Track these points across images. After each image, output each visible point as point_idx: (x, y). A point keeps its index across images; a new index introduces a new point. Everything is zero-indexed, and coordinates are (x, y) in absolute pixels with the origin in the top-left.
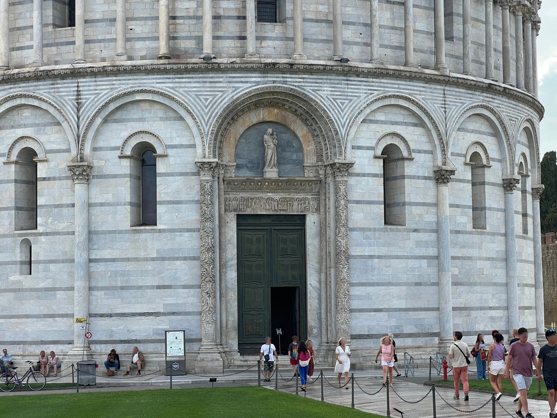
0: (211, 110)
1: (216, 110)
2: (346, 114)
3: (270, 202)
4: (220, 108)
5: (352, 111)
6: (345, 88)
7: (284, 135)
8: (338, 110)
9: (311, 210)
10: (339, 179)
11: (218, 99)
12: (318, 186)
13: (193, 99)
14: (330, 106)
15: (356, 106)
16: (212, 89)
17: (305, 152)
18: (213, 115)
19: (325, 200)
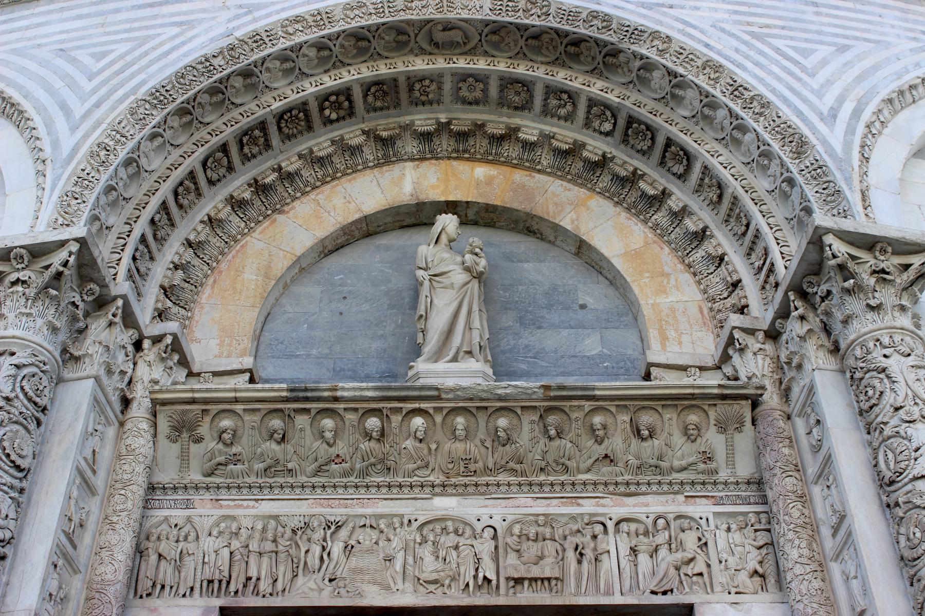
0: (115, 81)
1: (143, 76)
2: (829, 82)
3: (451, 540)
4: (161, 70)
5: (860, 79)
6: (803, 12)
7: (526, 265)
8: (784, 69)
9: (720, 577)
10: (864, 325)
11: (162, 44)
12: (744, 440)
13: (44, 64)
14: (737, 50)
15: (875, 68)
16: (136, 25)
17: (647, 311)
18: (120, 93)
19: (804, 498)
